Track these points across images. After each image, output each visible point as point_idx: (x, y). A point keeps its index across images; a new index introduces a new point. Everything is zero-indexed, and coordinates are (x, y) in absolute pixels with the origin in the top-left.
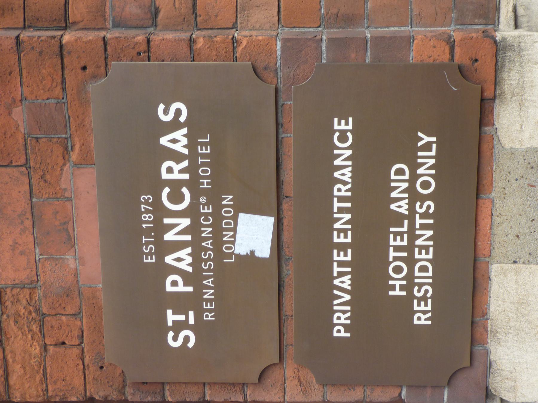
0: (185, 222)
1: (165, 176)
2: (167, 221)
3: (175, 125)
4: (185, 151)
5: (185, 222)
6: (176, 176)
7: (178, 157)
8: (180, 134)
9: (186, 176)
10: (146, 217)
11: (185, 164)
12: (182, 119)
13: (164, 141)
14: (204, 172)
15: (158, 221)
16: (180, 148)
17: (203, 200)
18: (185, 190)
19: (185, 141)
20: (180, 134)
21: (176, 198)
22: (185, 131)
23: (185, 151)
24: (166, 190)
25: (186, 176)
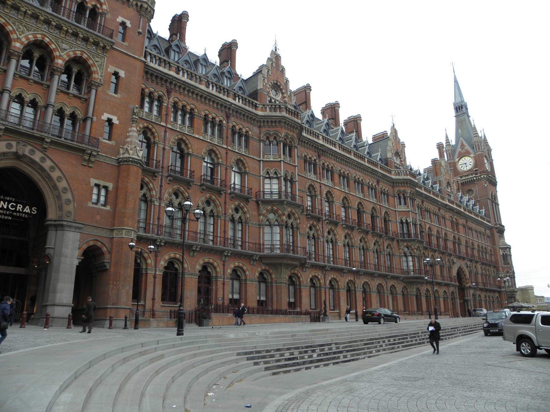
0: (5, 207)
1: (19, 205)
2: (6, 203)
3: (31, 210)
4: (24, 211)
5: (5, 207)
6: (18, 208)
7: (23, 209)
8: (29, 211)
9: (18, 210)
10: (8, 199)
11: (21, 210)
12: (32, 212)
13: (27, 207)
14: (18, 214)
15: (7, 201)
16: (25, 210)
17: (11, 212)
18: (14, 209)
19: (27, 212)
20: (29, 211)
21: (12, 206)
22: (29, 212)
23: (24, 211)
24: (15, 205)
25: (18, 210)
